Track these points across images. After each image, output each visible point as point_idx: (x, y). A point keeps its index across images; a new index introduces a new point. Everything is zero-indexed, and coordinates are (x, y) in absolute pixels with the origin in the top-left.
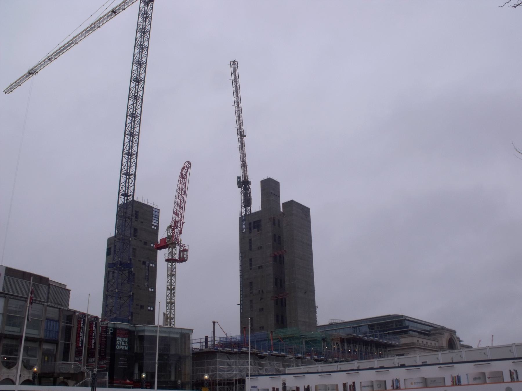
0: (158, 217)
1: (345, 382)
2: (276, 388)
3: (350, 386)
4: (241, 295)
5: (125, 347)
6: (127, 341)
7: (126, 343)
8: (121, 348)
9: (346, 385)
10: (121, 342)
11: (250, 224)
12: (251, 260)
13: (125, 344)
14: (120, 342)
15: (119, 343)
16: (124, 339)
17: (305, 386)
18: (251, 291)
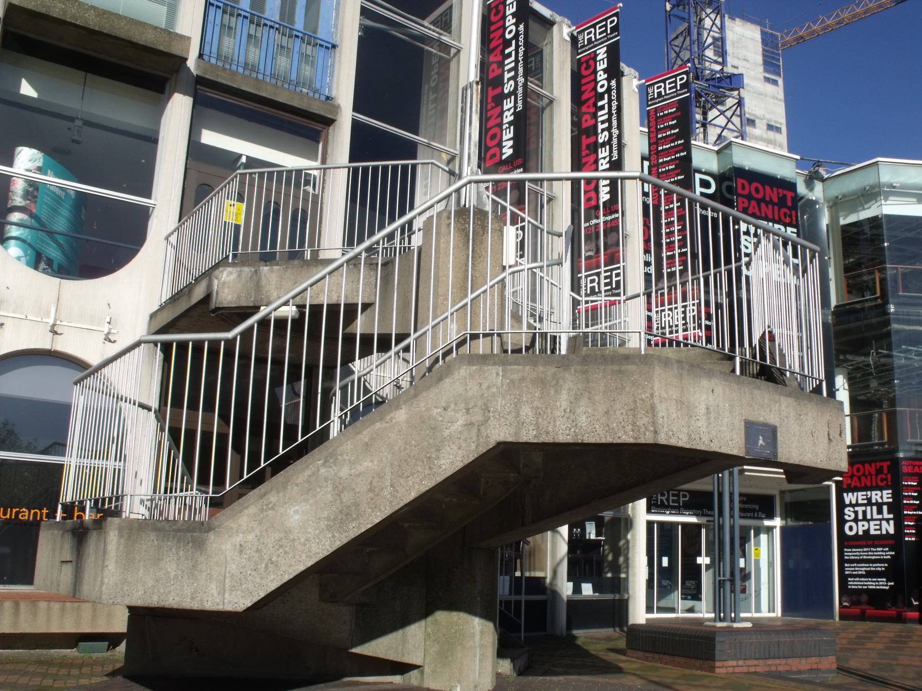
5: (880, 525)
6: (891, 500)
7: (885, 508)
8: (867, 532)
10: (864, 508)
13: (880, 512)
14: (856, 509)
15: (856, 513)
16: (876, 496)
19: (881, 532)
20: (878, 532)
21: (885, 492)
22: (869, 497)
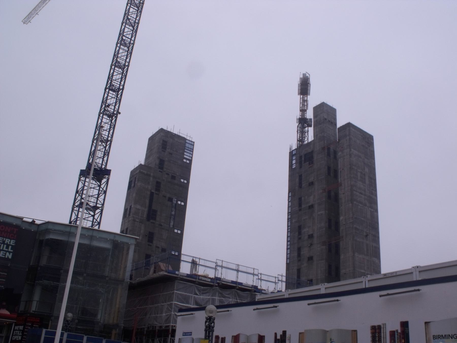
0: (192, 150)
1: (376, 324)
2: (221, 337)
3: (393, 334)
4: (288, 241)
5: (6, 254)
6: (14, 245)
7: (10, 247)
9: (380, 333)
11: (301, 157)
12: (300, 199)
13: (7, 247)
16: (7, 241)
17: (276, 334)
18: (300, 237)
19: (5, 257)
20: (4, 256)
21: (12, 241)
22: (4, 240)
